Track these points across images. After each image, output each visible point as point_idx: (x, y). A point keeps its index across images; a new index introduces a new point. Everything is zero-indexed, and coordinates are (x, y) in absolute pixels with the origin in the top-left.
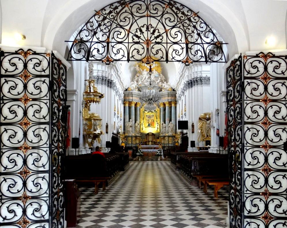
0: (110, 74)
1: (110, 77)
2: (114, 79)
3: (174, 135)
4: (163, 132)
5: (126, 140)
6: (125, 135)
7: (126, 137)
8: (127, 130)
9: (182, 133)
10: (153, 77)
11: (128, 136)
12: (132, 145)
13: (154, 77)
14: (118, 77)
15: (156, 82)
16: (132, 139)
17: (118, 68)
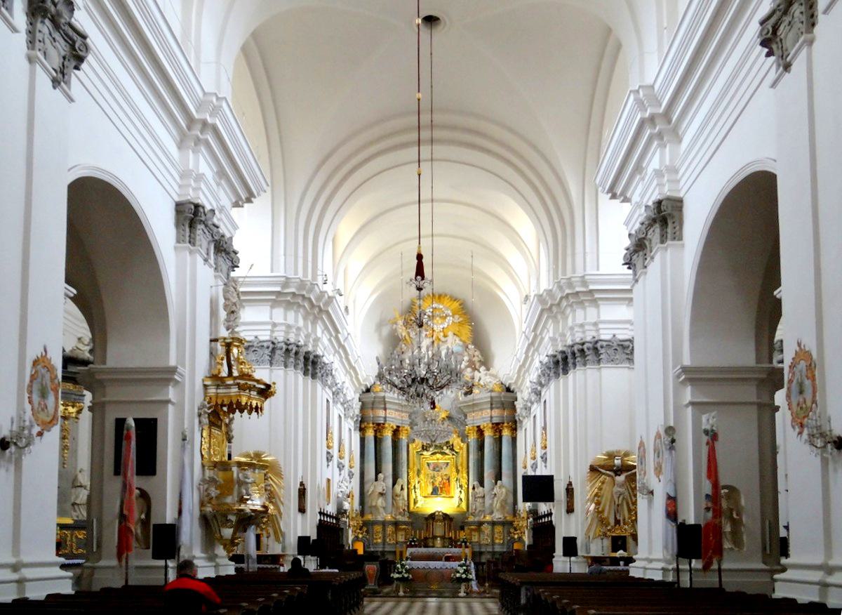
3: (508, 518)
4: (476, 510)
9: (534, 513)
14: (341, 351)
17: (339, 319)
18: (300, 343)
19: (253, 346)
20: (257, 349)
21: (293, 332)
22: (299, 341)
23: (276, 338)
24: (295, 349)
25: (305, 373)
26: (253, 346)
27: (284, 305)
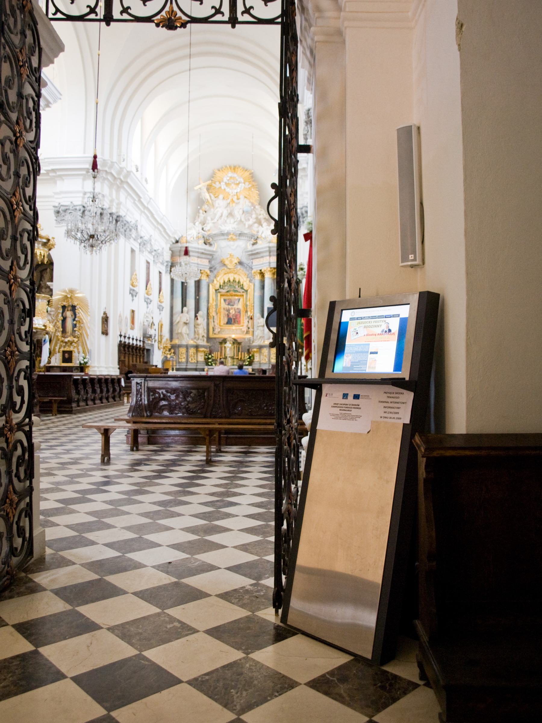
5: (174, 353)
6: (173, 343)
7: (174, 348)
8: (176, 332)
10: (239, 212)
11: (180, 346)
12: (187, 366)
13: (241, 212)
15: (245, 225)
16: (187, 351)
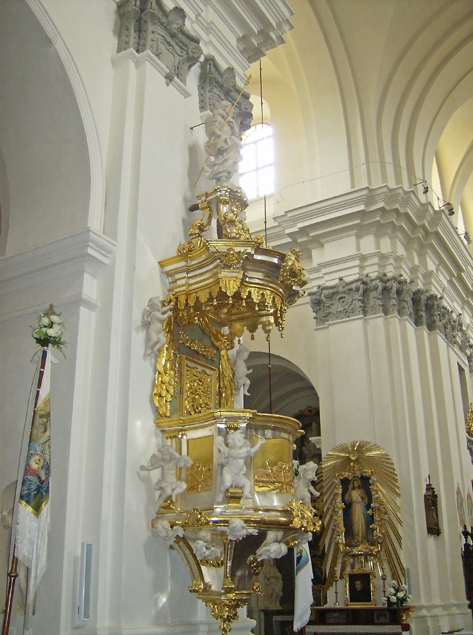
0: (422, 270)
1: (420, 284)
2: (445, 296)
18: (402, 278)
19: (337, 293)
20: (343, 295)
21: (391, 264)
22: (401, 275)
23: (367, 276)
24: (395, 286)
25: (417, 322)
26: (337, 293)
27: (374, 229)
